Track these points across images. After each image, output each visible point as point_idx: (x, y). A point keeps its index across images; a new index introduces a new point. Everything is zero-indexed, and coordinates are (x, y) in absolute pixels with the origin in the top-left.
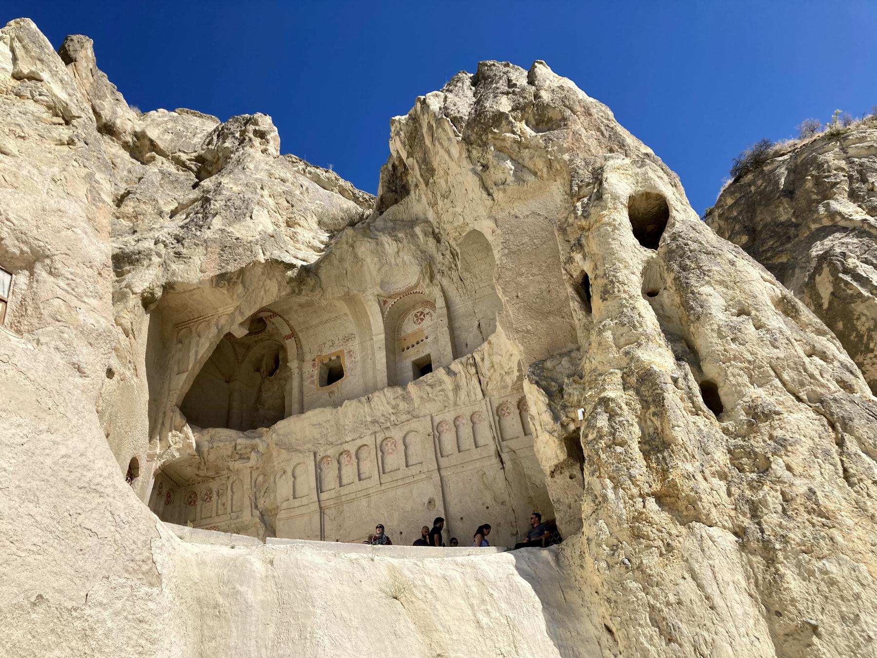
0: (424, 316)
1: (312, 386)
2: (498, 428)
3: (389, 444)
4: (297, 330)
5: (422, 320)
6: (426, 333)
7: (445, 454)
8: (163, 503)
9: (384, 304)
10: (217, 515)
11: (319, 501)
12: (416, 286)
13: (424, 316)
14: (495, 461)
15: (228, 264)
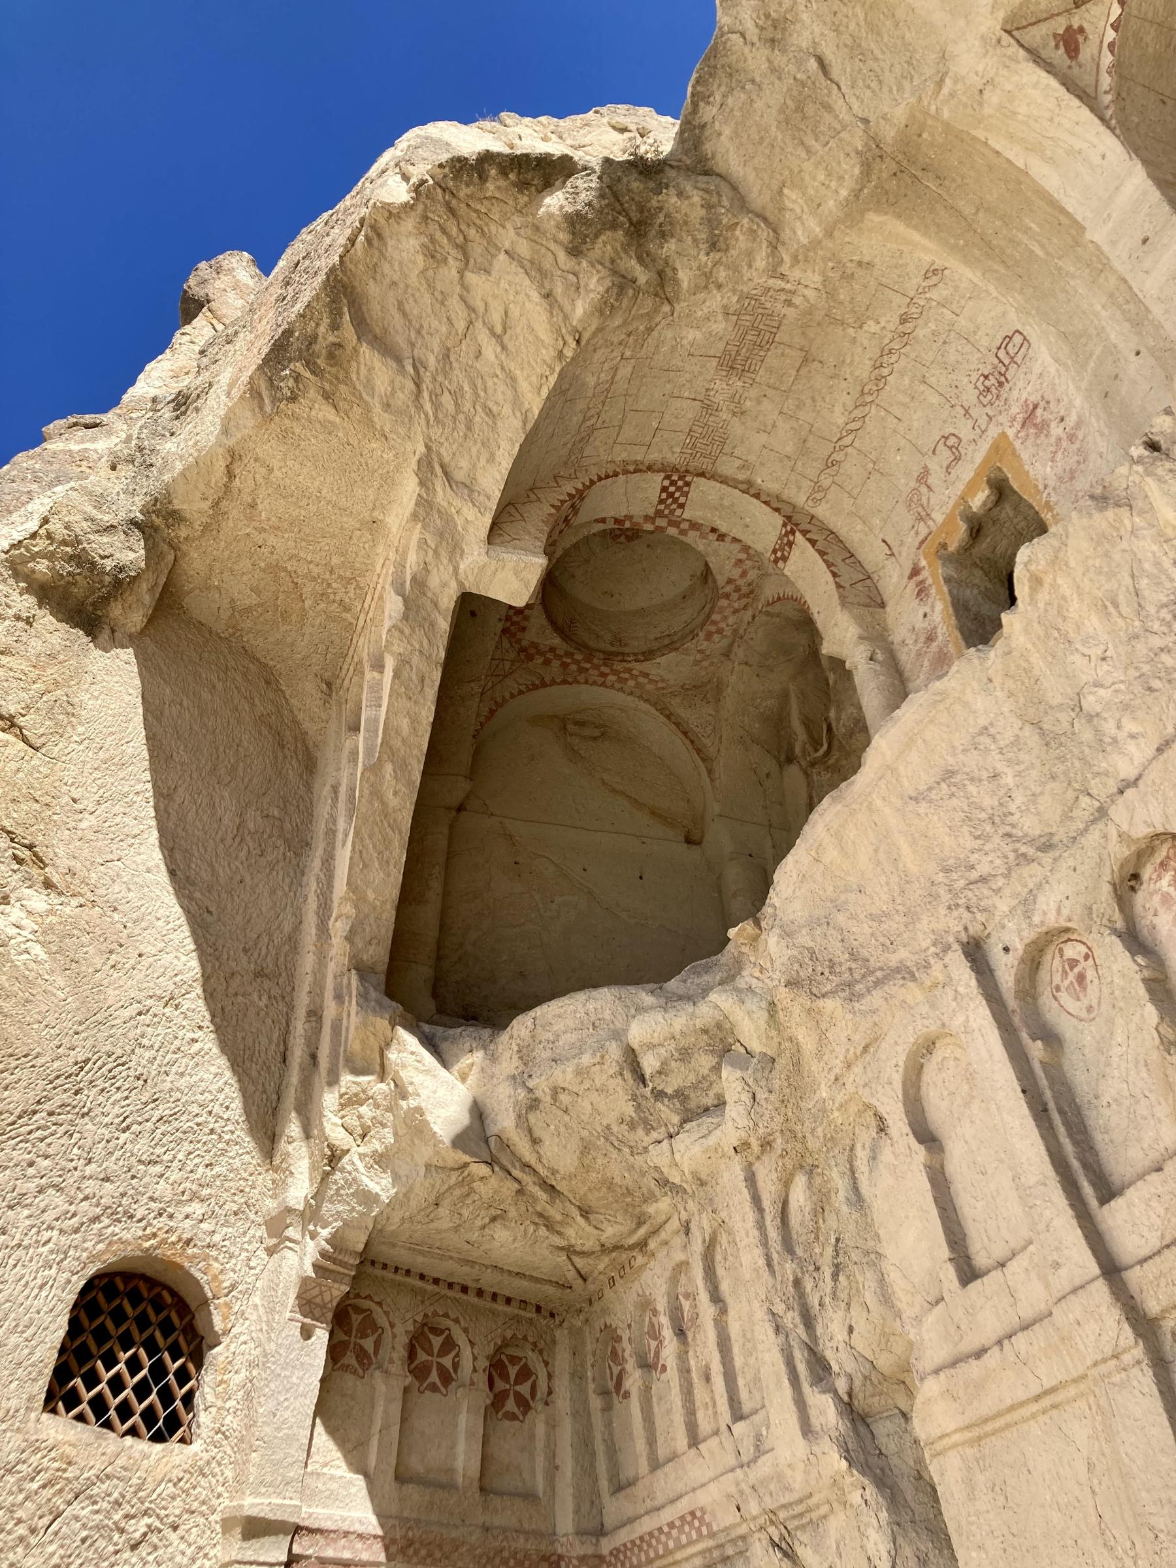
4: (800, 499)
10: (694, 1440)
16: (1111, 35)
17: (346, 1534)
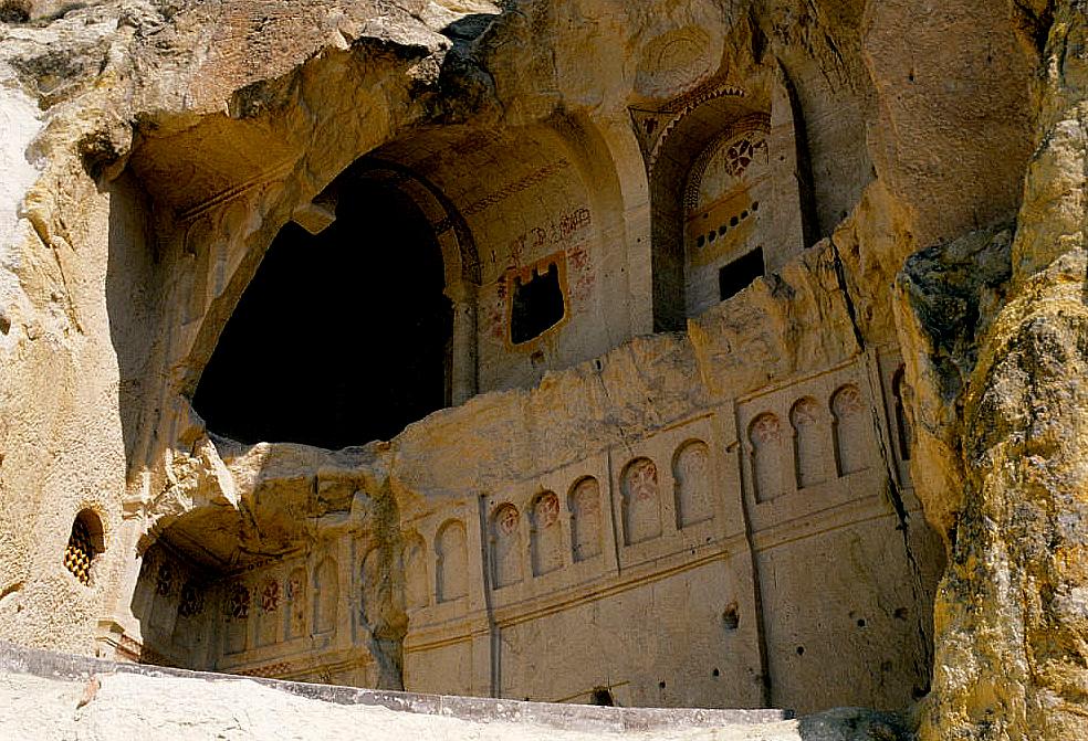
0: (751, 153)
1: (496, 341)
2: (895, 426)
3: (641, 474)
5: (745, 162)
6: (753, 194)
7: (766, 494)
8: (173, 610)
9: (649, 131)
11: (489, 608)
12: (721, 77)
13: (751, 153)
14: (883, 508)
15: (267, 60)
16: (665, 133)
17: (132, 640)
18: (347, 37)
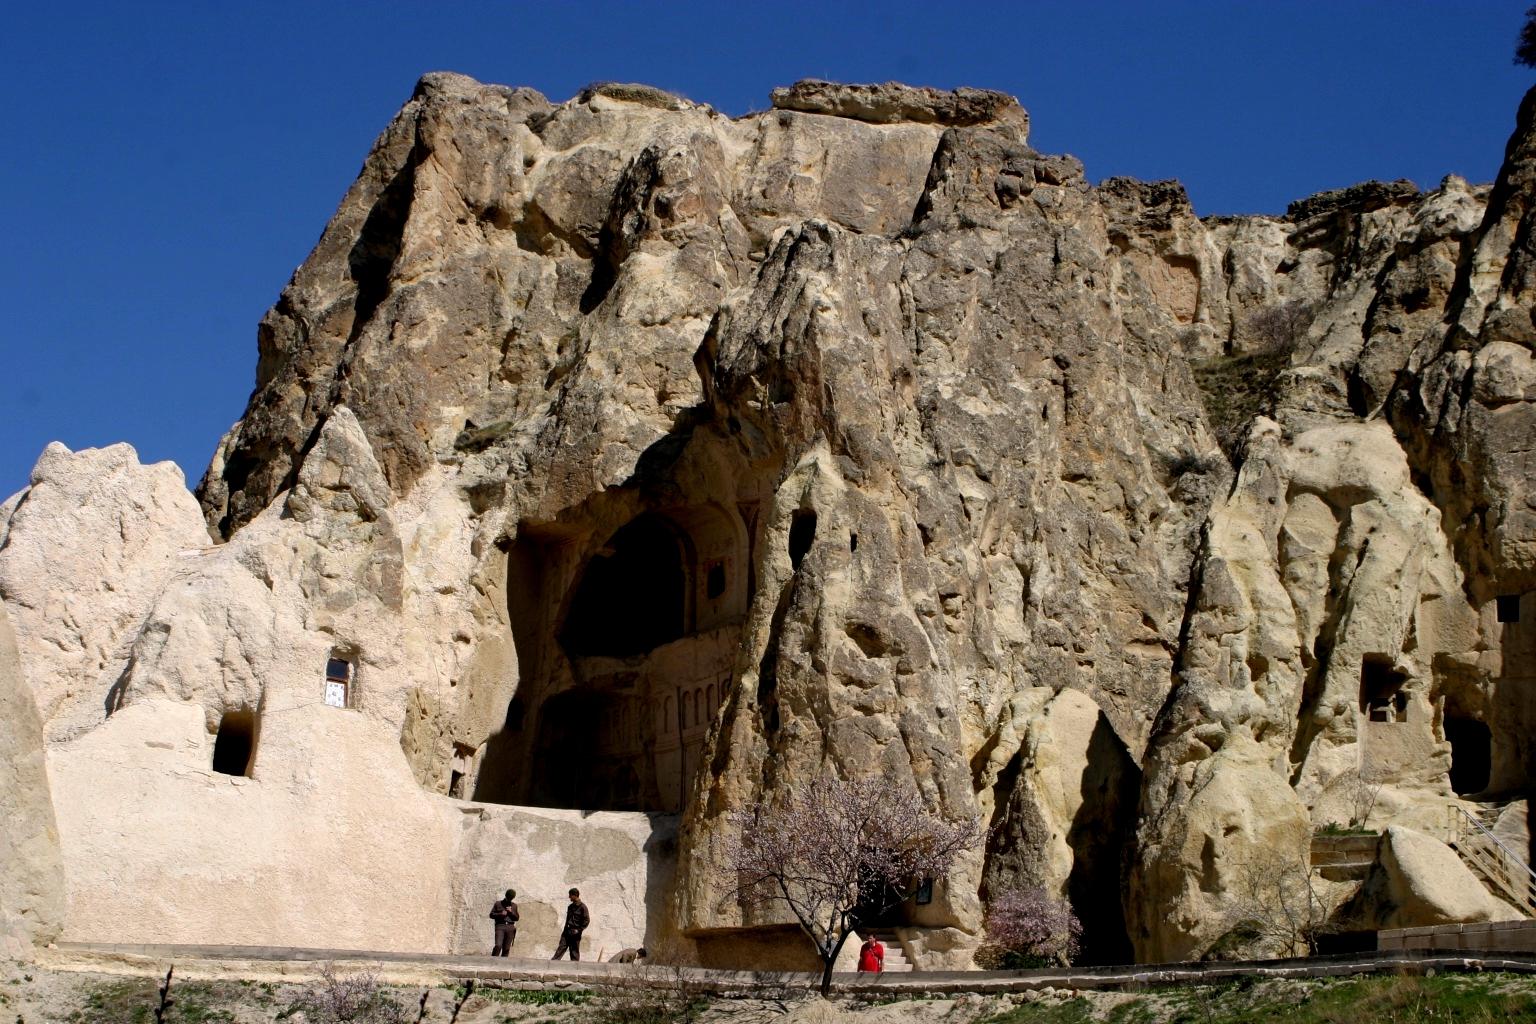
18: (604, 486)
